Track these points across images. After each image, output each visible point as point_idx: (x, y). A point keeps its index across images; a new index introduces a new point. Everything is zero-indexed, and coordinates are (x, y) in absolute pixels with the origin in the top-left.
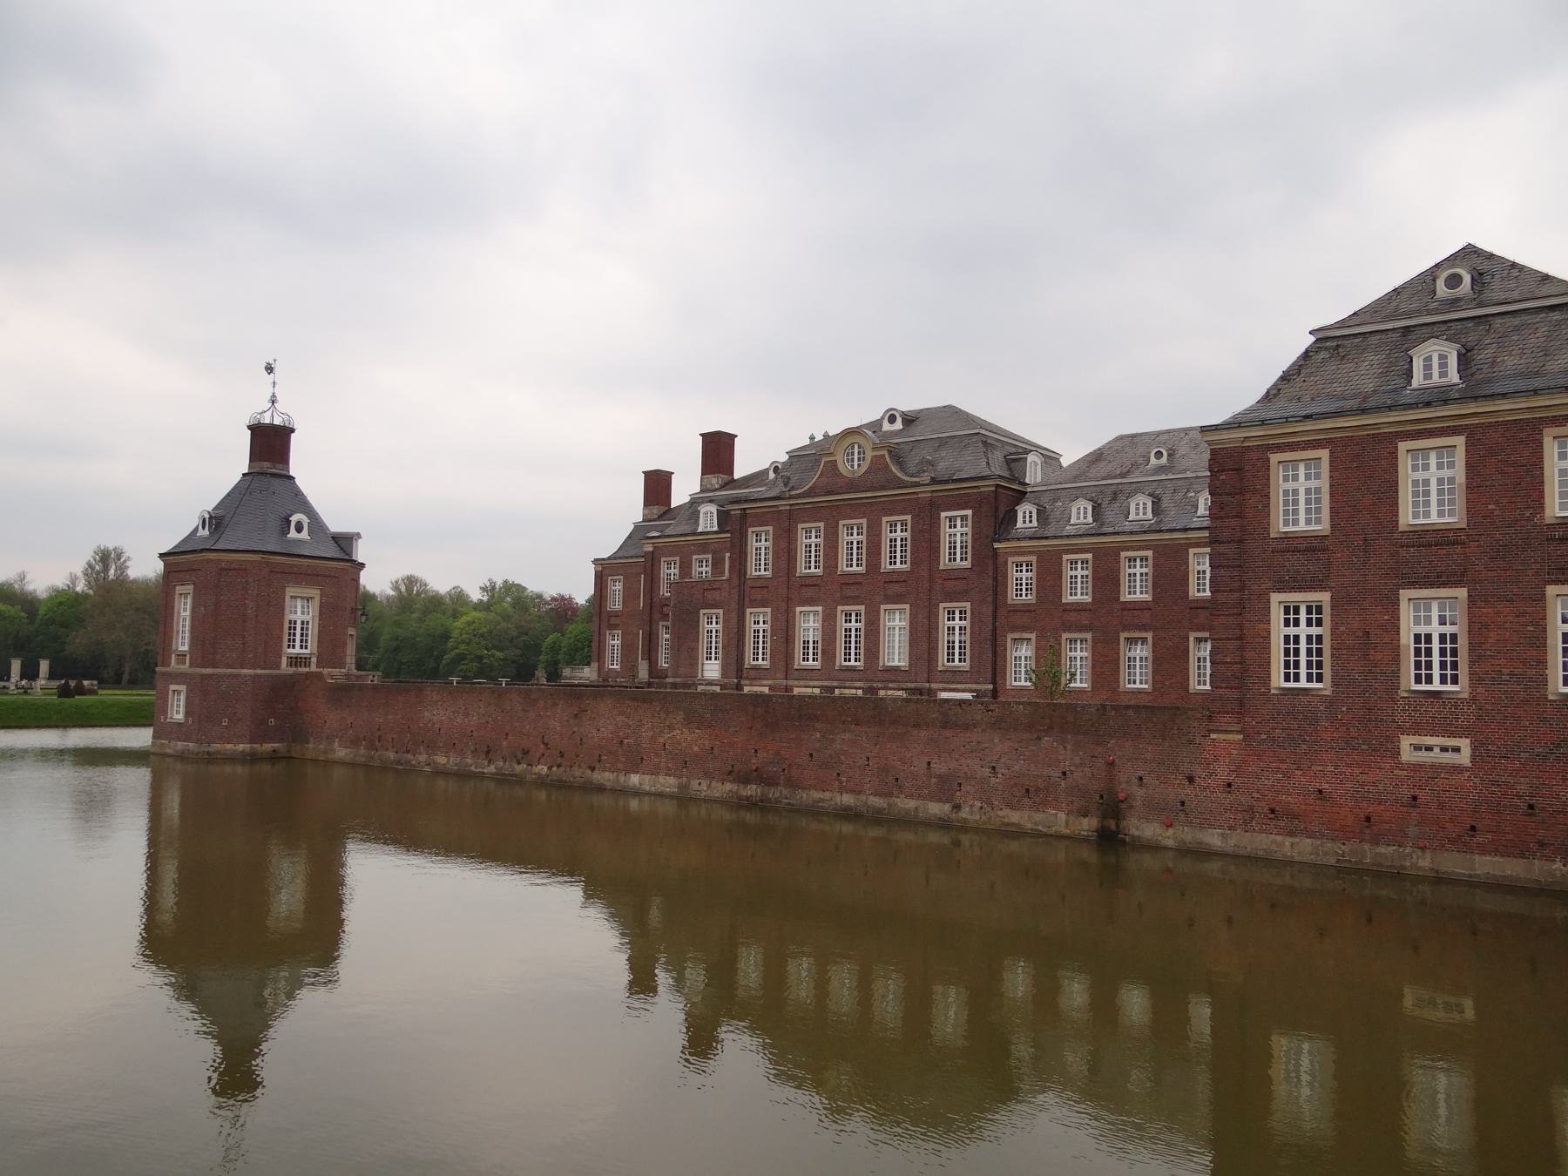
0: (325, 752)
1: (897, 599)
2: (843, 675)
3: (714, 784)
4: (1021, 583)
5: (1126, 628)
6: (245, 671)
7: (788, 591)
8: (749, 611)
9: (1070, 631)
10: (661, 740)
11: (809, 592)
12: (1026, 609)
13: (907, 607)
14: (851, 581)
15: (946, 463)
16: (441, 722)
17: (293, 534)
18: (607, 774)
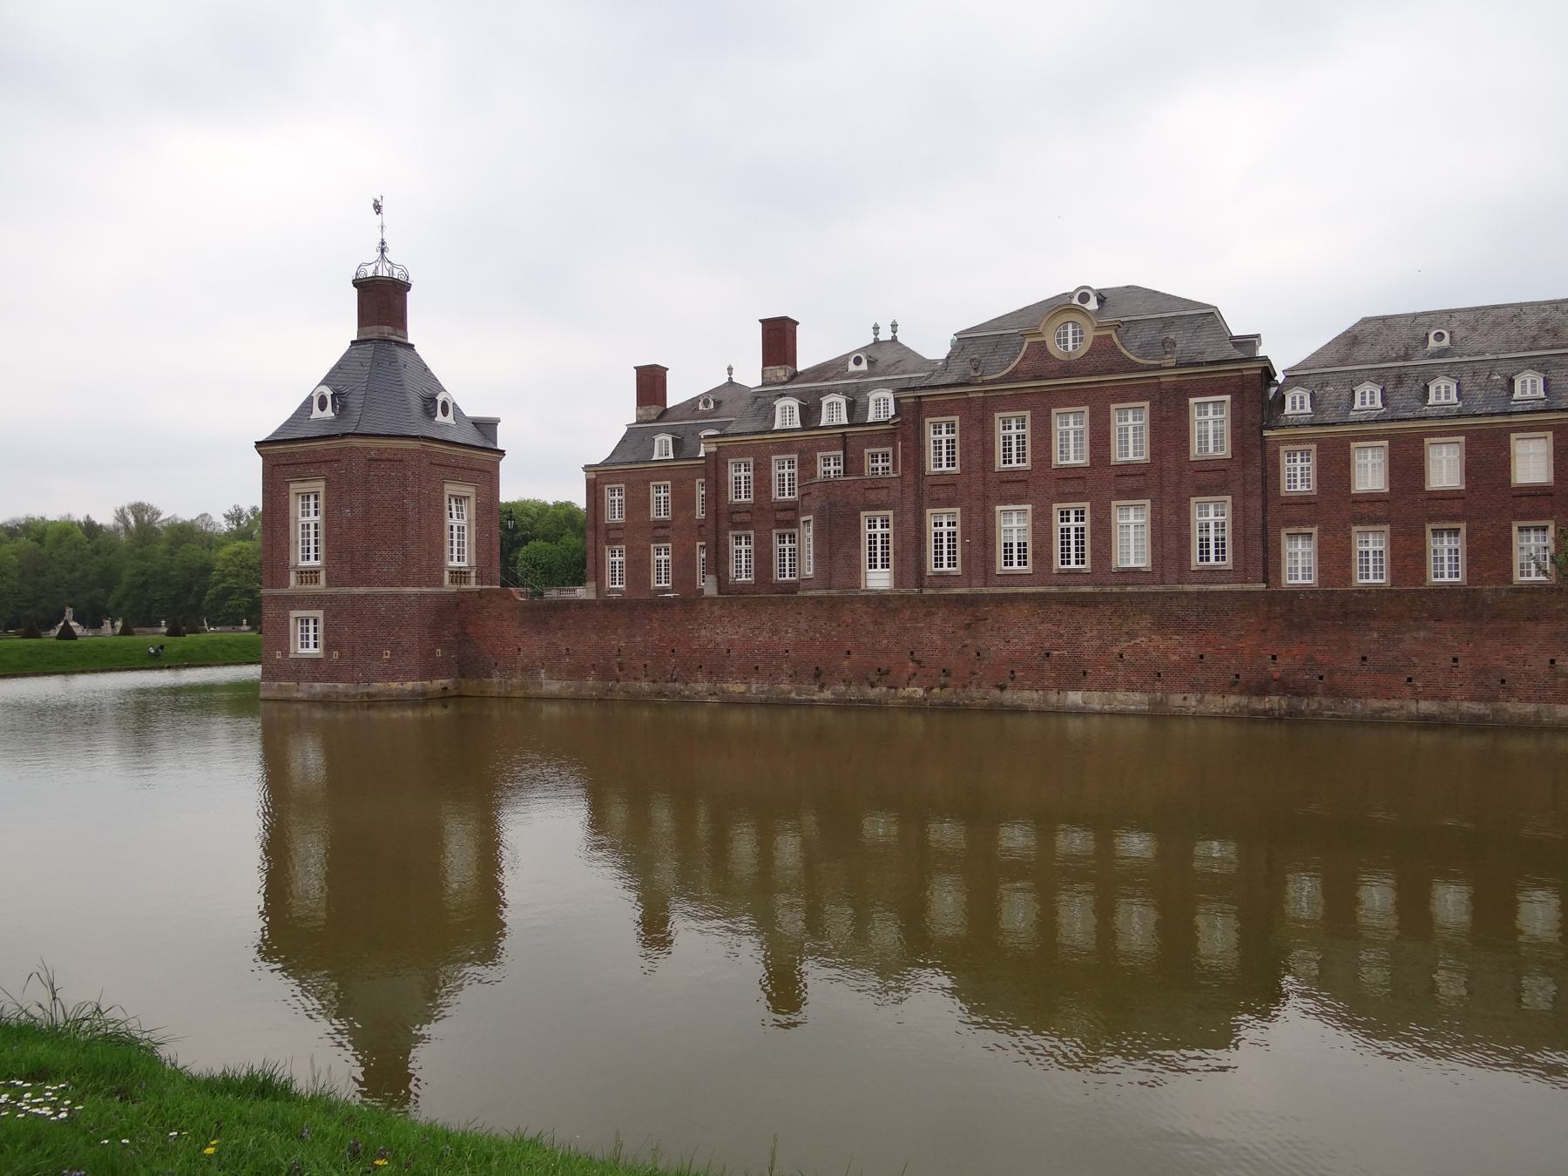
0: (523, 687)
1: (1135, 494)
2: (1063, 580)
3: (1208, 697)
4: (1298, 474)
5: (1433, 519)
6: (408, 589)
7: (980, 489)
8: (929, 511)
9: (1361, 524)
10: (1116, 650)
11: (1013, 489)
12: (1301, 501)
13: (1148, 502)
14: (1070, 475)
15: (1185, 343)
16: (731, 643)
17: (440, 418)
18: (1027, 694)
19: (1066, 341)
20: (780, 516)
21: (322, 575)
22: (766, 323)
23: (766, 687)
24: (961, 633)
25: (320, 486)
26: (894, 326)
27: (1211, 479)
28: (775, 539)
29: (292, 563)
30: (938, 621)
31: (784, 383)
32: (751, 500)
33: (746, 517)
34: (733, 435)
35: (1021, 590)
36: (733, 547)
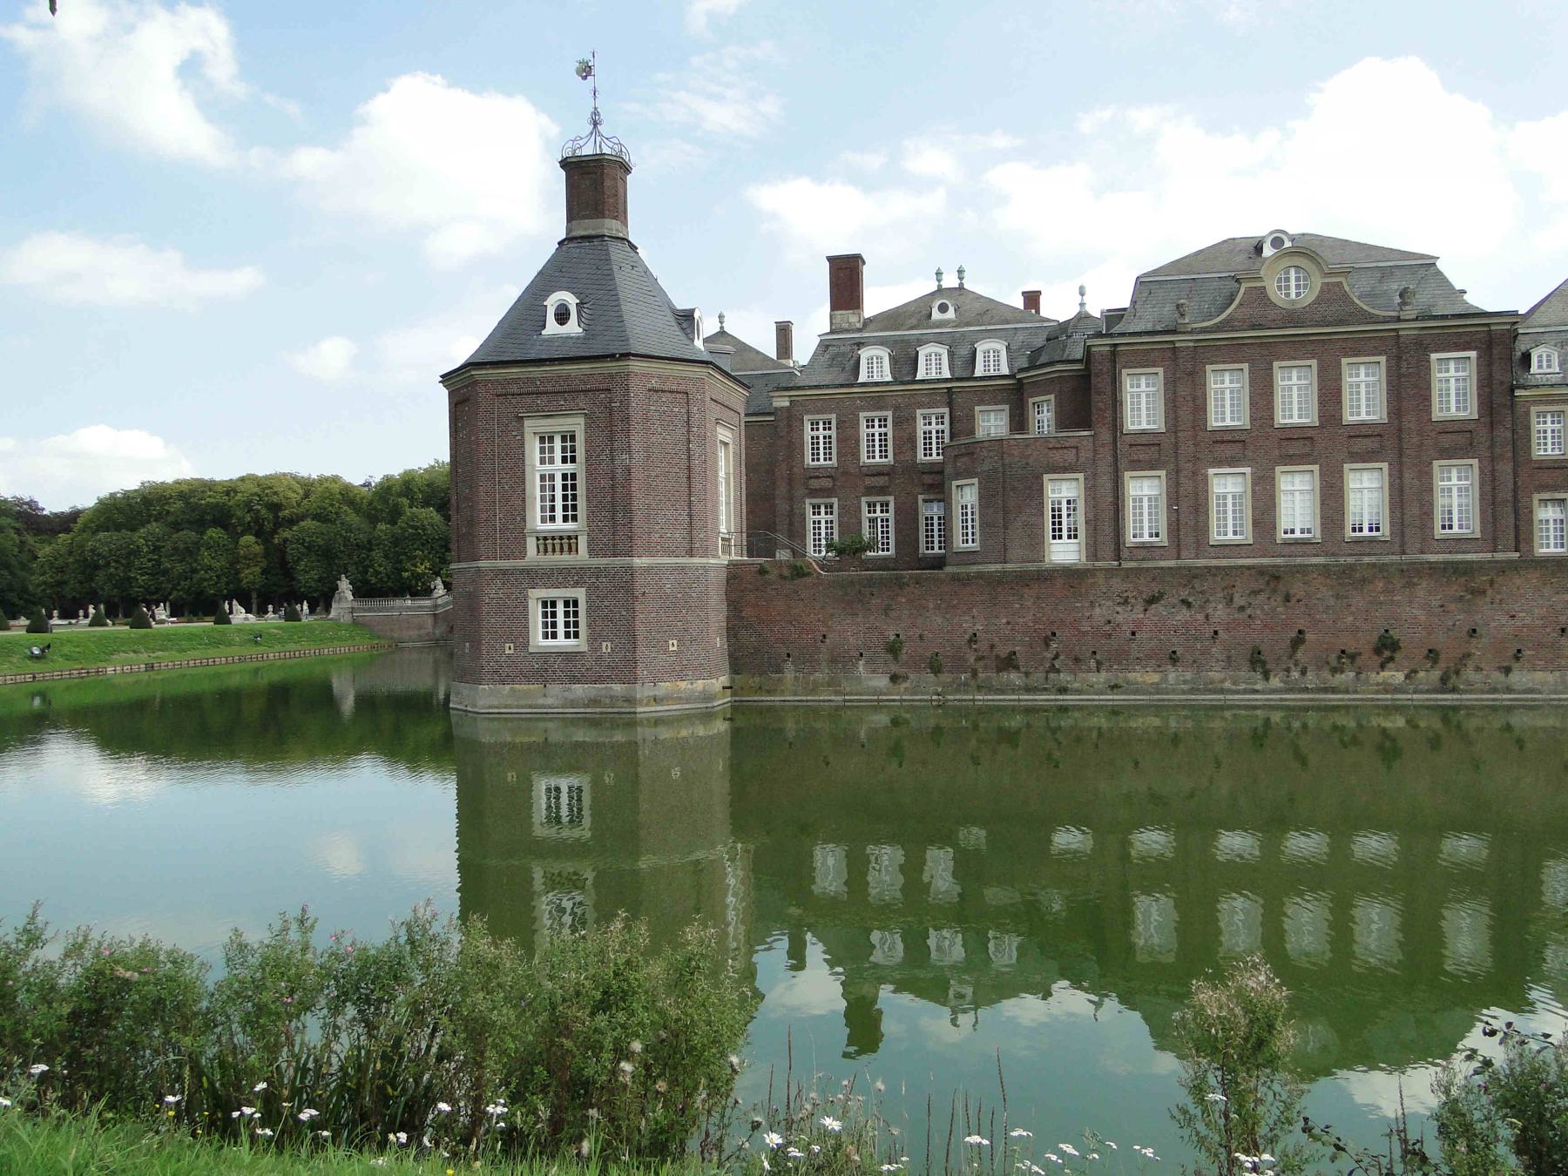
7: (1186, 449)
11: (1229, 450)
13: (1385, 466)
18: (1539, 676)
19: (1287, 288)
20: (869, 481)
21: (583, 543)
22: (832, 260)
23: (1188, 676)
24: (1452, 607)
25: (577, 425)
26: (960, 272)
27: (1456, 441)
28: (865, 508)
29: (529, 526)
30: (1421, 593)
31: (859, 330)
32: (834, 462)
33: (827, 483)
34: (811, 388)
35: (1241, 562)
36: (811, 517)
